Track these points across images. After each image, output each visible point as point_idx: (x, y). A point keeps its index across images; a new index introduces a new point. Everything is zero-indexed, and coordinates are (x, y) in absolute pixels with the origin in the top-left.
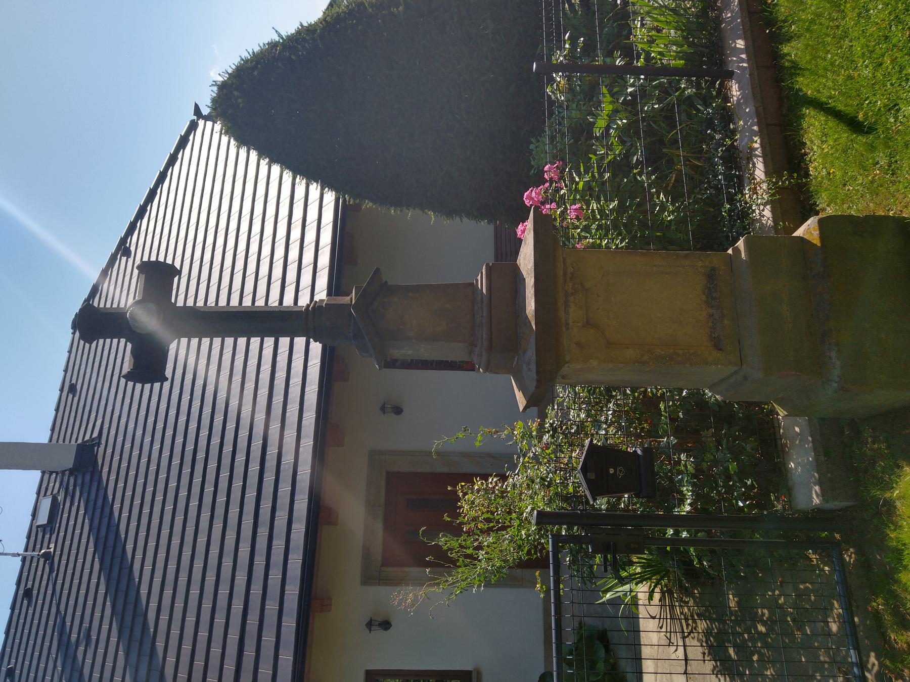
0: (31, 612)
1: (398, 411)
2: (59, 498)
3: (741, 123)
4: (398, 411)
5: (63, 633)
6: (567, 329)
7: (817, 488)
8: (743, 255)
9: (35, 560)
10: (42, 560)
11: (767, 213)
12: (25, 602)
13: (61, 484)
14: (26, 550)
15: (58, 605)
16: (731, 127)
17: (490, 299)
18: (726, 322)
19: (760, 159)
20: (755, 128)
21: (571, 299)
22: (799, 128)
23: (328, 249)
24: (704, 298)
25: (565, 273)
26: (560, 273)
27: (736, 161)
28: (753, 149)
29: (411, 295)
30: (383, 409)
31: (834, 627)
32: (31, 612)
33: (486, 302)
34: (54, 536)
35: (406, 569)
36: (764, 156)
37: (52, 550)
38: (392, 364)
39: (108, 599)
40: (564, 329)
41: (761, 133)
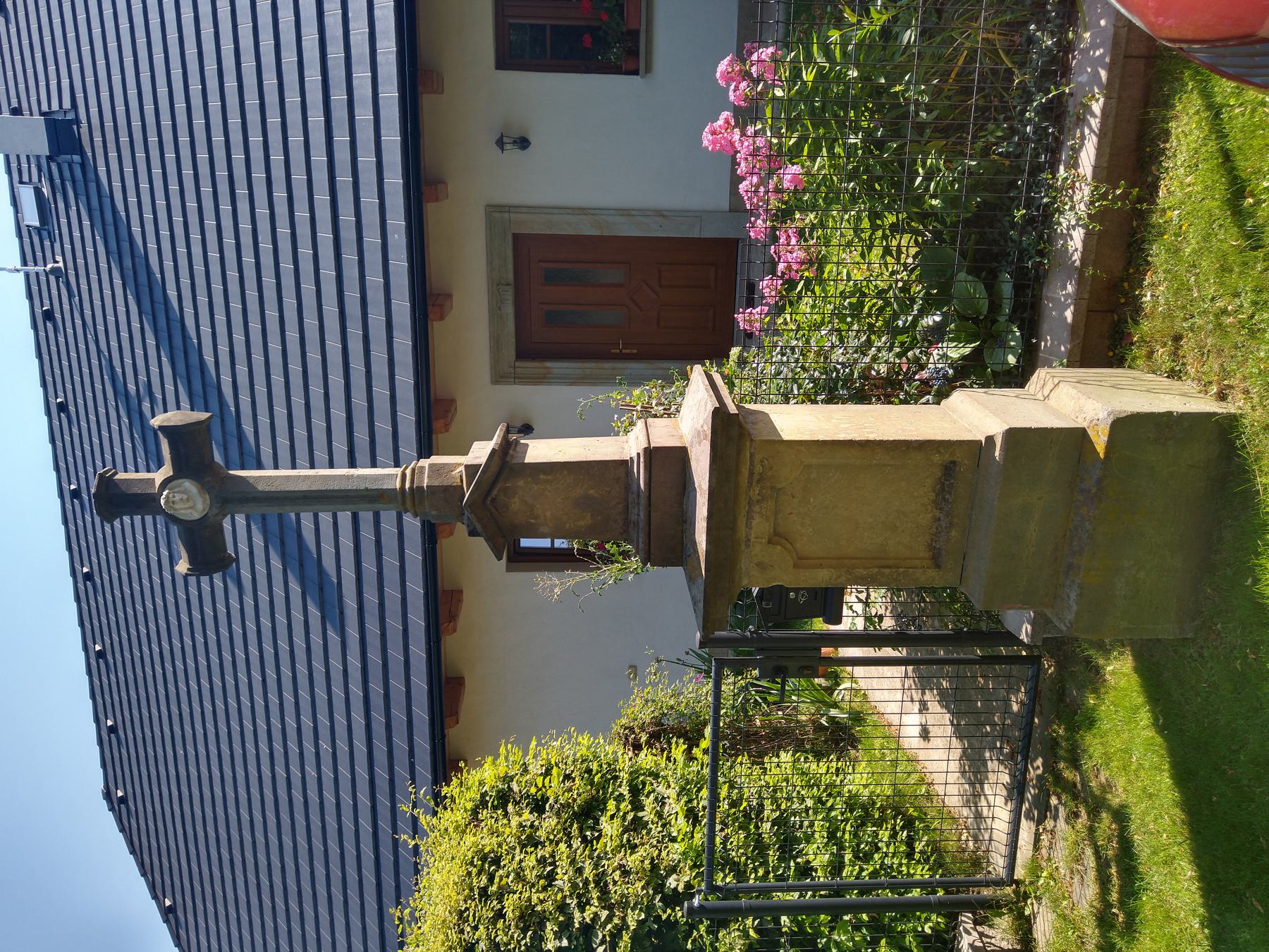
0: (61, 339)
1: (523, 143)
2: (45, 190)
3: (1087, 35)
4: (523, 143)
5: (121, 393)
6: (748, 546)
7: (1029, 627)
8: (997, 454)
9: (43, 278)
10: (52, 278)
11: (1078, 236)
12: (49, 325)
13: (40, 170)
14: (25, 263)
15: (99, 351)
16: (1070, 35)
17: (649, 497)
18: (953, 533)
19: (1095, 139)
20: (1103, 74)
21: (757, 508)
22: (1167, 104)
23: (410, 396)
24: (932, 496)
25: (751, 474)
26: (745, 471)
27: (1060, 115)
28: (1088, 108)
29: (542, 477)
30: (500, 143)
31: (1015, 707)
32: (61, 339)
33: (643, 501)
34: (57, 245)
35: (548, 364)
36: (1101, 136)
37: (61, 265)
38: (522, 559)
39: (162, 353)
40: (743, 547)
41: (1108, 90)
